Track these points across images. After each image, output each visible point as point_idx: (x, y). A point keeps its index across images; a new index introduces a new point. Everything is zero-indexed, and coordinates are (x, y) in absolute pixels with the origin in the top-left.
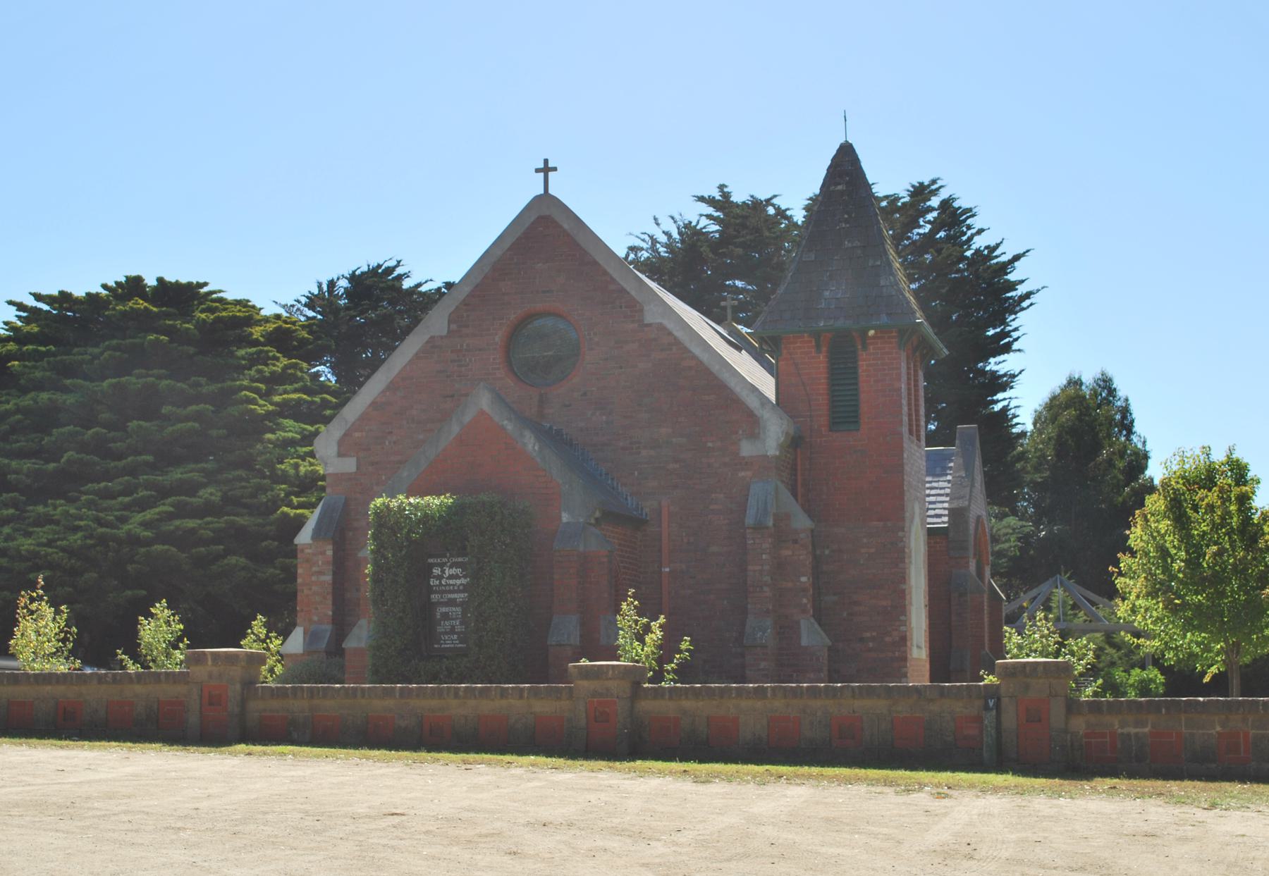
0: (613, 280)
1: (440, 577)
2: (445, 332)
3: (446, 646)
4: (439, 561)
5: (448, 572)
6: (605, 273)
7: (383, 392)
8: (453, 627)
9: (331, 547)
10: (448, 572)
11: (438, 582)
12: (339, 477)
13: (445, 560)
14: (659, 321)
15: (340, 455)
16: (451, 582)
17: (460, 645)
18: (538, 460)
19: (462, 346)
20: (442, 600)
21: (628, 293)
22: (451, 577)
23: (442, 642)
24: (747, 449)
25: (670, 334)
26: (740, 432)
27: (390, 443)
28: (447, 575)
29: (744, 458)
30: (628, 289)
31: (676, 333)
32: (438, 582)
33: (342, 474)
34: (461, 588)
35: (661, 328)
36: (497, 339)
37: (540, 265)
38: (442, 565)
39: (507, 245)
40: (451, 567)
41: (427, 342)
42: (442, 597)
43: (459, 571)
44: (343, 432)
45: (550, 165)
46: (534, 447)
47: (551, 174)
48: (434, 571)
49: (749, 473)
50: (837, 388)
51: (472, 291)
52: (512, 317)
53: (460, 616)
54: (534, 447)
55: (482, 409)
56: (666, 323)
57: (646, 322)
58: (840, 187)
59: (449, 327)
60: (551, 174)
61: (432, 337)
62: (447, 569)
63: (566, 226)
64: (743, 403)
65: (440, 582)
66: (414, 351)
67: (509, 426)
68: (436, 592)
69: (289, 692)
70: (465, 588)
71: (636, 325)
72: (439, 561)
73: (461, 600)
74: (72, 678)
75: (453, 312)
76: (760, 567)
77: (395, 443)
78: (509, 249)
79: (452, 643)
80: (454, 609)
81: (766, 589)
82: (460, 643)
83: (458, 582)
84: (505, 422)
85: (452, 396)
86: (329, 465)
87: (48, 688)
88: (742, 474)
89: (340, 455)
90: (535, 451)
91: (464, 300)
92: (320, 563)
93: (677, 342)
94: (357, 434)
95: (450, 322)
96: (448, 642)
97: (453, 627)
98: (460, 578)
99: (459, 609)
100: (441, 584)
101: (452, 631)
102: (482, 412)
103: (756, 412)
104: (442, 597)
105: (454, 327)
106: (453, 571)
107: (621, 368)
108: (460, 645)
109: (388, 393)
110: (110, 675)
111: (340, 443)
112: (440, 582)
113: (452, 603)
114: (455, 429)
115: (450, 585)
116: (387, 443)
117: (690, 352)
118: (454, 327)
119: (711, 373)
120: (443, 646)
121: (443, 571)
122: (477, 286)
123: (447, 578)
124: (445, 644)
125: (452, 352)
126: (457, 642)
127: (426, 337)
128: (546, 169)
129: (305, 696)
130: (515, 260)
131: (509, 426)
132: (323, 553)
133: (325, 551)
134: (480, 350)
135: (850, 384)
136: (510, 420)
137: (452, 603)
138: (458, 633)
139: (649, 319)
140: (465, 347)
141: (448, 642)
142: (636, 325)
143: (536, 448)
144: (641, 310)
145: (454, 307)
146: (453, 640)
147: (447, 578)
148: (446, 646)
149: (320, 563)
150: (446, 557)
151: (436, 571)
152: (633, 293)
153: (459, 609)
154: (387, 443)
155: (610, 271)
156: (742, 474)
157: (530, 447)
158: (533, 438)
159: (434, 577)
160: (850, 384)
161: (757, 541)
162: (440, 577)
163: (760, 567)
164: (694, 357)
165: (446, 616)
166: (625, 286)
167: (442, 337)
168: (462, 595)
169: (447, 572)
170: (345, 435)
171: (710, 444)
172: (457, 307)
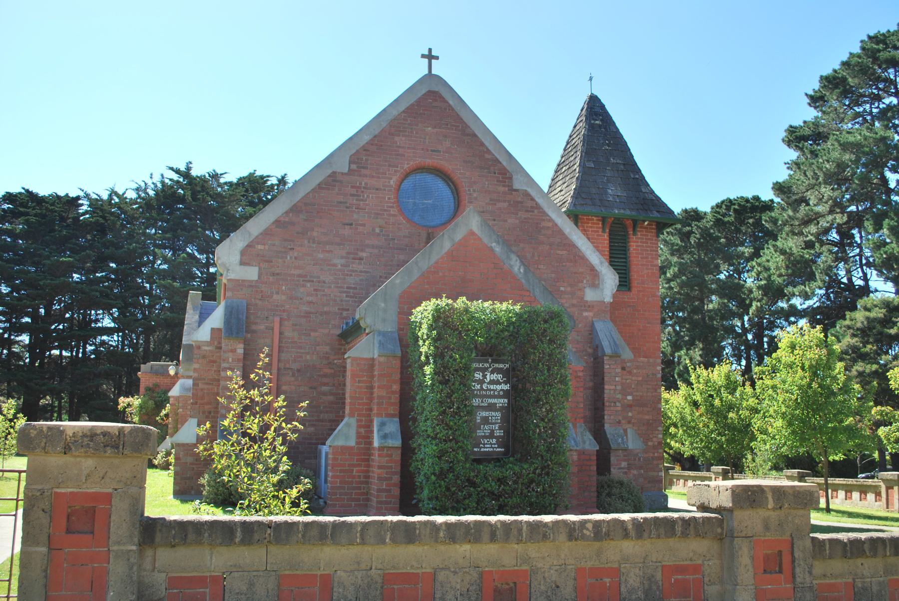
0: (489, 152)
1: (481, 382)
2: (346, 170)
3: (485, 450)
4: (481, 365)
5: (489, 377)
6: (482, 144)
7: (287, 213)
8: (492, 431)
9: (242, 346)
10: (489, 377)
11: (479, 387)
12: (239, 284)
13: (486, 365)
14: (525, 188)
15: (242, 263)
16: (492, 387)
17: (499, 450)
18: (523, 281)
19: (361, 184)
20: (483, 404)
21: (501, 163)
22: (492, 382)
23: (481, 445)
24: (590, 295)
25: (533, 199)
26: (585, 282)
27: (291, 258)
28: (488, 380)
29: (587, 302)
30: (501, 160)
31: (537, 200)
32: (479, 387)
33: (243, 281)
34: (501, 393)
35: (527, 194)
36: (392, 182)
37: (429, 129)
38: (484, 370)
39: (402, 108)
40: (492, 372)
41: (329, 176)
42: (482, 402)
43: (500, 377)
44: (246, 244)
45: (427, 53)
46: (519, 269)
47: (433, 61)
48: (476, 375)
49: (591, 314)
50: (622, 256)
51: (371, 140)
52: (406, 166)
53: (499, 421)
54: (519, 269)
55: (471, 230)
56: (530, 190)
57: (514, 188)
58: (597, 122)
59: (349, 166)
60: (433, 61)
61: (334, 173)
62: (489, 374)
63: (451, 102)
64: (587, 260)
65: (481, 387)
66: (318, 182)
67: (498, 249)
68: (477, 396)
69: (866, 547)
70: (506, 394)
71: (507, 189)
72: (481, 365)
73: (501, 405)
74: (520, 530)
75: (353, 155)
76: (613, 387)
77: (296, 258)
78: (404, 112)
79: (491, 447)
80: (493, 413)
81: (618, 404)
82: (498, 447)
83: (499, 387)
84: (494, 244)
85: (351, 224)
86: (230, 271)
87: (465, 548)
88: (585, 314)
89: (242, 263)
90: (520, 272)
91: (363, 146)
92: (230, 360)
93: (538, 207)
94: (260, 247)
95: (350, 163)
96: (488, 446)
97: (492, 431)
98: (500, 384)
99: (498, 414)
100: (482, 389)
101: (491, 435)
102: (472, 233)
103: (597, 268)
104: (482, 402)
105: (354, 167)
106: (495, 377)
107: (494, 220)
108: (499, 450)
109: (291, 215)
110: (589, 526)
111: (243, 253)
112: (481, 387)
113: (491, 407)
114: (447, 245)
115: (490, 390)
116: (289, 258)
117: (548, 216)
118: (354, 167)
119: (564, 234)
120: (482, 450)
121: (485, 376)
122: (375, 137)
123: (488, 383)
124: (485, 448)
125: (352, 187)
126: (496, 446)
127: (330, 172)
128: (430, 57)
129: (888, 554)
130: (409, 121)
131: (498, 249)
132: (234, 351)
133: (235, 349)
134: (377, 189)
135: (621, 258)
136: (498, 243)
137: (491, 407)
138: (496, 437)
139: (516, 186)
140: (363, 185)
141: (488, 446)
142: (507, 189)
143: (522, 270)
144: (511, 178)
145: (354, 151)
146: (491, 444)
147: (488, 383)
148: (485, 450)
149: (230, 360)
150: (488, 362)
151: (478, 376)
152: (504, 163)
153: (498, 414)
154: (289, 258)
155: (487, 144)
156: (585, 314)
157: (516, 269)
158: (518, 261)
159: (475, 381)
160: (621, 258)
161: (612, 367)
162: (481, 382)
163: (613, 387)
164: (551, 220)
165: (486, 421)
166: (498, 157)
167: (342, 174)
168: (502, 401)
169: (488, 377)
170: (248, 246)
171: (562, 289)
172: (357, 151)
